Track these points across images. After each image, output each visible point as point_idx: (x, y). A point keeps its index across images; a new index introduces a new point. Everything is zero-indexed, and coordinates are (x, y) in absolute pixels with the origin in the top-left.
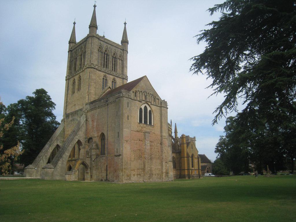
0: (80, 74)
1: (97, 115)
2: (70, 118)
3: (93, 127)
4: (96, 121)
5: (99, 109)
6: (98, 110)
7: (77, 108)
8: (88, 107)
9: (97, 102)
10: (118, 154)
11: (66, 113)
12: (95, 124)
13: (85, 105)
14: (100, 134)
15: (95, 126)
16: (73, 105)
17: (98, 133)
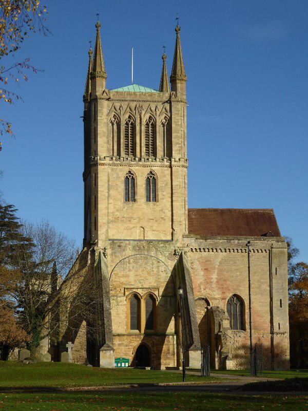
0: (153, 168)
1: (220, 263)
2: (129, 252)
3: (208, 282)
4: (217, 273)
5: (224, 254)
6: (222, 255)
7: (150, 236)
8: (193, 242)
9: (221, 241)
10: (281, 331)
11: (107, 237)
12: (214, 277)
13: (181, 237)
14: (229, 295)
15: (214, 280)
16: (134, 225)
17: (224, 293)
